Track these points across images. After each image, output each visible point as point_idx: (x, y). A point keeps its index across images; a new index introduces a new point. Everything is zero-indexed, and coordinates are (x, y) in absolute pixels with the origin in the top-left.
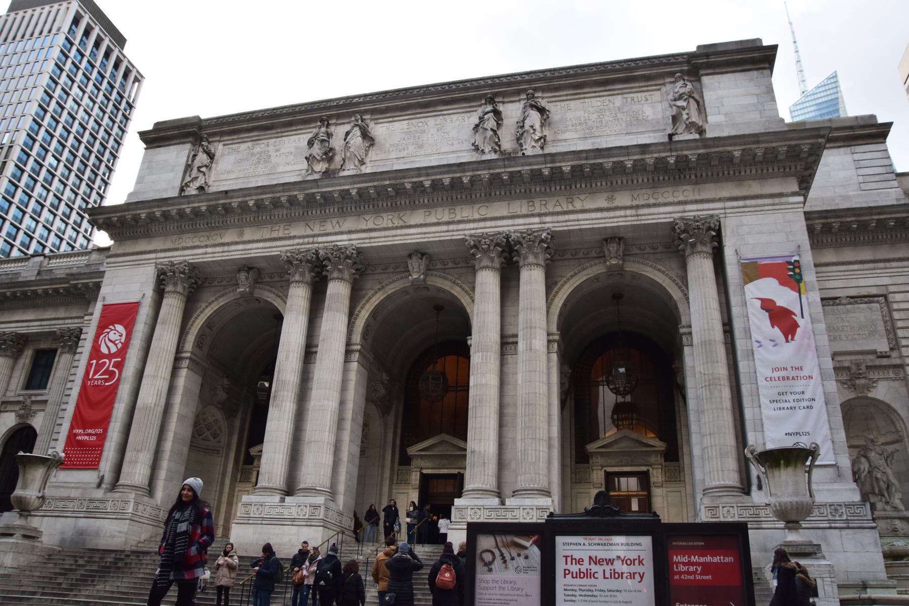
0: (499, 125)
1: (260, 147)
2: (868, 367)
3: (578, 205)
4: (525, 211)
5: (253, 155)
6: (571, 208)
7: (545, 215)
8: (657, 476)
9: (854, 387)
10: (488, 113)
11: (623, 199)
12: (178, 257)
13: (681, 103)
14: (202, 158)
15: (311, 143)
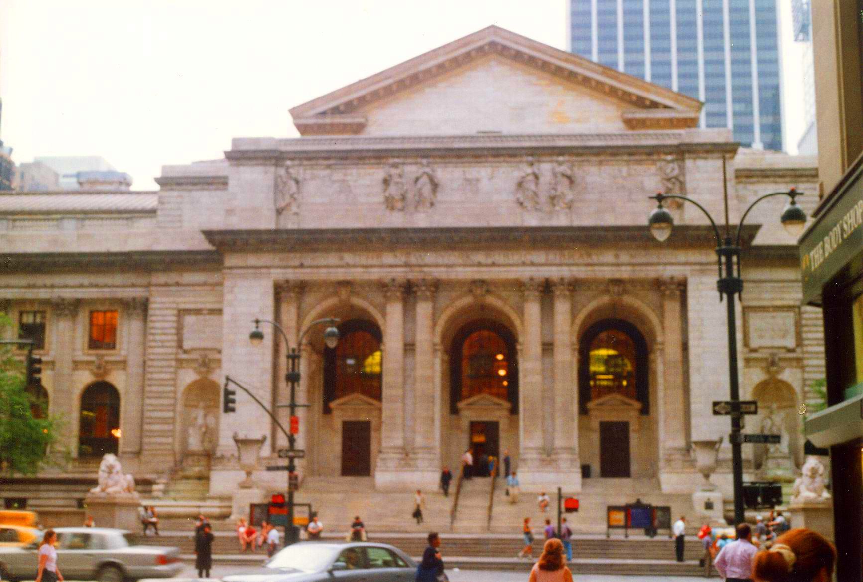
0: (537, 184)
1: (338, 175)
2: (780, 359)
3: (594, 259)
4: (557, 261)
5: (334, 182)
6: (590, 261)
7: (573, 265)
8: (633, 427)
9: (768, 371)
10: (528, 175)
11: (625, 257)
12: (292, 275)
13: (670, 185)
14: (292, 184)
15: (386, 182)
